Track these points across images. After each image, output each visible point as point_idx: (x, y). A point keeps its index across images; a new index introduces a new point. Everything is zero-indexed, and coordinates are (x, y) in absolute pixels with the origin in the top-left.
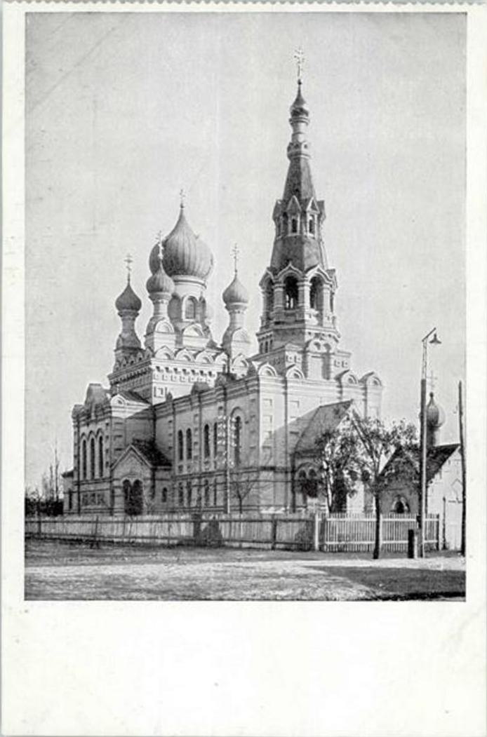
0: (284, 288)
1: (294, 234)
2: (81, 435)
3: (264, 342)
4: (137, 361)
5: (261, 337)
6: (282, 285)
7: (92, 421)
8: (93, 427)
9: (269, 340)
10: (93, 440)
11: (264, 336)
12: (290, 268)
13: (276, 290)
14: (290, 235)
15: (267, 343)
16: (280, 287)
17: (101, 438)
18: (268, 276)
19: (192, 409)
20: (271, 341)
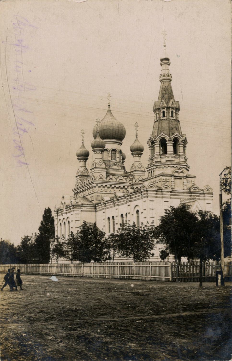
0: (159, 144)
1: (163, 118)
2: (59, 220)
3: (150, 172)
4: (87, 181)
5: (149, 169)
6: (158, 143)
7: (64, 213)
8: (65, 216)
9: (152, 171)
10: (65, 223)
11: (150, 168)
12: (162, 135)
13: (155, 146)
14: (162, 119)
15: (151, 172)
16: (158, 144)
17: (69, 222)
18: (152, 139)
19: (115, 206)
20: (154, 171)
